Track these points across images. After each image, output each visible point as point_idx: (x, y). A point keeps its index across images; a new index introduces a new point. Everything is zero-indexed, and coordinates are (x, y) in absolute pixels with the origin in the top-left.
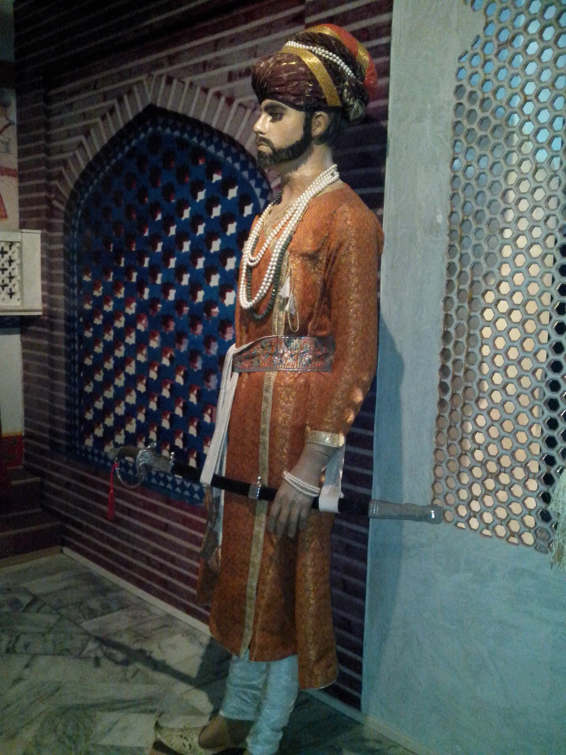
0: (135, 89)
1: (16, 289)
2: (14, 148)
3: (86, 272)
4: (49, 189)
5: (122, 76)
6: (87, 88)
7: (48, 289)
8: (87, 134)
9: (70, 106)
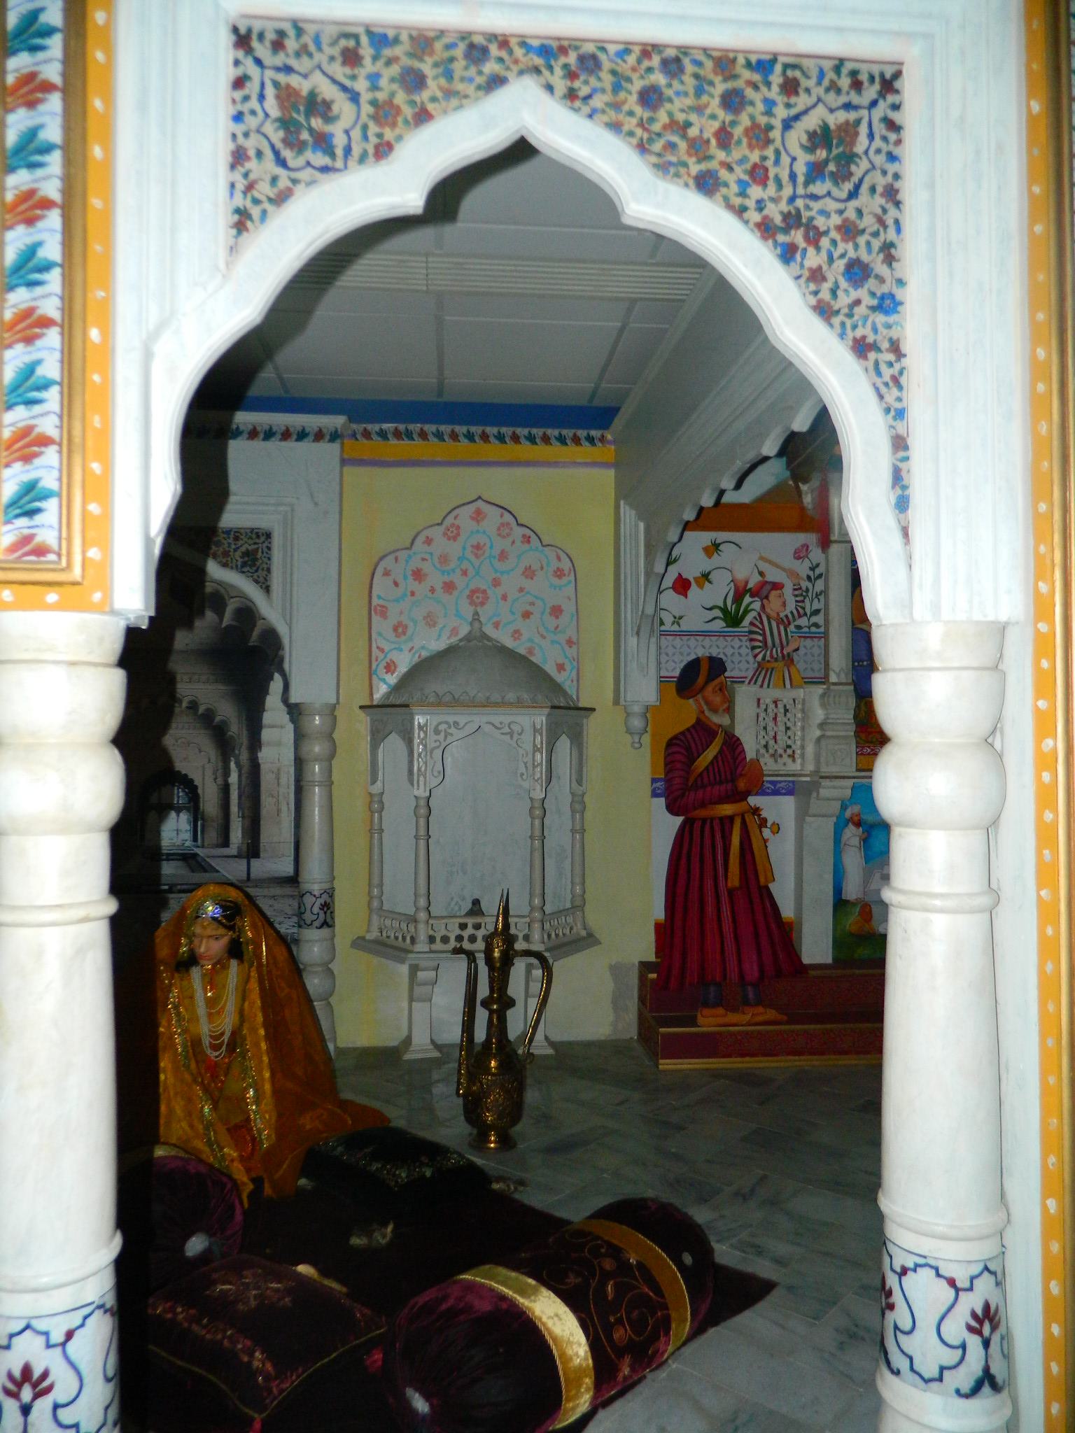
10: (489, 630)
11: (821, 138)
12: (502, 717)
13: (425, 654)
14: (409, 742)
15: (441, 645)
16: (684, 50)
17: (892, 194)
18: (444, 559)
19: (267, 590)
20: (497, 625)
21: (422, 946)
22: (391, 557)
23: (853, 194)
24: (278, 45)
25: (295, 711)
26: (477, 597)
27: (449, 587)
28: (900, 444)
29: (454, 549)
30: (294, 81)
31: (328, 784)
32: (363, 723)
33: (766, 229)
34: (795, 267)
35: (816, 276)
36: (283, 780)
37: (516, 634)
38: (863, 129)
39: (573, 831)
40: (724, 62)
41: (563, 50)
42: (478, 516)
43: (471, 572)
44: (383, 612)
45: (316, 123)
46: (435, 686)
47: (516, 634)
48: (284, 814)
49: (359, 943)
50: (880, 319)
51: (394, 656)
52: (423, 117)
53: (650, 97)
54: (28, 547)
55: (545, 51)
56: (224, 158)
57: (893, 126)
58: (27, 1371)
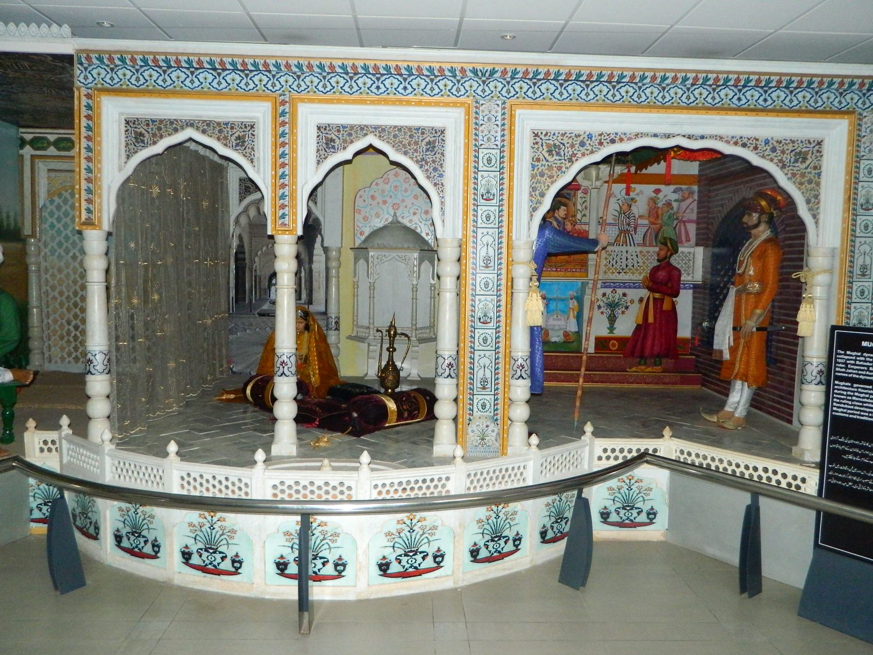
9: (717, 195)
10: (400, 219)
12: (402, 253)
13: (375, 228)
14: (367, 262)
15: (381, 225)
17: (443, 154)
19: (316, 203)
20: (403, 218)
21: (371, 337)
25: (326, 250)
26: (396, 206)
27: (385, 202)
29: (387, 187)
32: (351, 254)
33: (417, 162)
35: (427, 170)
37: (411, 221)
40: (410, 129)
44: (359, 212)
46: (378, 241)
47: (411, 221)
49: (350, 338)
51: (363, 229)
52: (352, 142)
53: (395, 136)
54: (284, 224)
55: (375, 128)
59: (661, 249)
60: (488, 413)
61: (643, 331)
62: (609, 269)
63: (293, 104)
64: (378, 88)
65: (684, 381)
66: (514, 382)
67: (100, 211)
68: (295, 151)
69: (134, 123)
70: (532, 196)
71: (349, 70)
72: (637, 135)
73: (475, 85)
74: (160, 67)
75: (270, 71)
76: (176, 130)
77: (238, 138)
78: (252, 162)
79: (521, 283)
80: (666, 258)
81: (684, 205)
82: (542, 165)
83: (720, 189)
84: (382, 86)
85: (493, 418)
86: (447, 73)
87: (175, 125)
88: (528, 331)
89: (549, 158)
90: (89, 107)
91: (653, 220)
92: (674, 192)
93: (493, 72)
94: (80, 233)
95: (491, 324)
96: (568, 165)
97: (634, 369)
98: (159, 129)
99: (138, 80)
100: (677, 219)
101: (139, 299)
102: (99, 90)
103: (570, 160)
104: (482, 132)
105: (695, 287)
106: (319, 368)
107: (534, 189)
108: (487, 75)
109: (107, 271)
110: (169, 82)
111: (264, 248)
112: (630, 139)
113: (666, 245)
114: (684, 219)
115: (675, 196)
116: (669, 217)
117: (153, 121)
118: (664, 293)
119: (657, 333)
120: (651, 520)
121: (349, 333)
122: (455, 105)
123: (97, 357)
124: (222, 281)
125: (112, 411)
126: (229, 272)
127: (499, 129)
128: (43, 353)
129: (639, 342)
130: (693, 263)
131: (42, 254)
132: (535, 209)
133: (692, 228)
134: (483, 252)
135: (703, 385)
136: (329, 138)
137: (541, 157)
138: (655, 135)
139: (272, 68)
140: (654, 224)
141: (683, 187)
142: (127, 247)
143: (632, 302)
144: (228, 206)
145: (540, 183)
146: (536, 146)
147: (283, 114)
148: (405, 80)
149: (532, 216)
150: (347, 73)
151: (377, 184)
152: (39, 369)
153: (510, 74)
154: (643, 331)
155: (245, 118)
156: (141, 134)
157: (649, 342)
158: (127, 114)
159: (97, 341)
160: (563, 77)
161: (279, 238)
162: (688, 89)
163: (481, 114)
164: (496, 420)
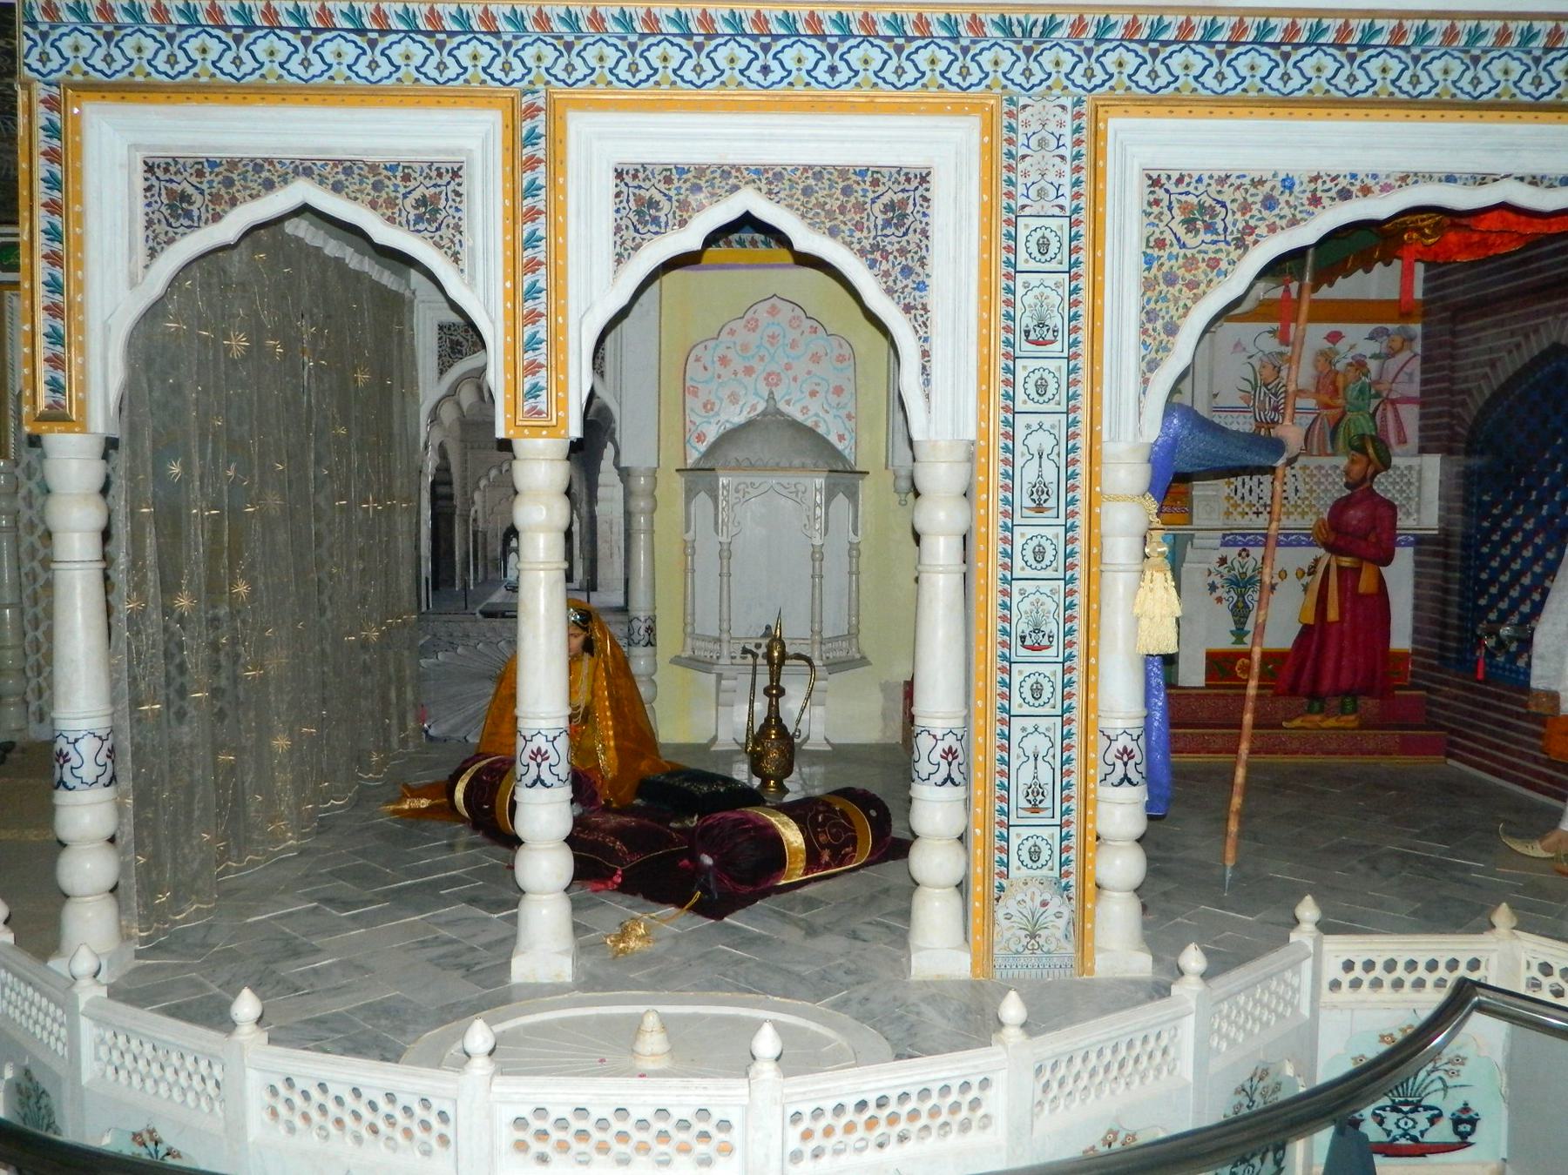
0: (1542, 330)
1: (1413, 509)
2: (1417, 378)
3: (1486, 493)
4: (1452, 415)
5: (1528, 317)
6: (1495, 325)
7: (1446, 509)
8: (1493, 364)
9: (1477, 341)
10: (782, 406)
11: (890, 207)
12: (789, 479)
13: (729, 426)
15: (739, 419)
16: (824, 167)
18: (745, 348)
20: (788, 403)
21: (725, 660)
22: (701, 346)
23: (905, 234)
24: (635, 177)
25: (625, 474)
26: (772, 379)
27: (749, 371)
28: (925, 354)
29: (753, 338)
30: (642, 192)
31: (651, 532)
32: (679, 483)
33: (862, 253)
34: (876, 271)
35: (887, 274)
36: (615, 529)
38: (911, 201)
39: (850, 573)
40: (843, 172)
41: (766, 171)
42: (773, 311)
43: (767, 358)
45: (652, 212)
46: (736, 454)
47: (805, 410)
48: (616, 557)
49: (677, 661)
50: (917, 293)
51: (704, 428)
53: (807, 191)
55: (757, 172)
56: (612, 230)
57: (926, 199)
58: (539, 749)
59: (1353, 462)
60: (1045, 871)
61: (1316, 637)
62: (1236, 506)
63: (554, 111)
64: (765, 70)
65: (1407, 748)
66: (1107, 792)
67: (83, 386)
68: (559, 229)
69: (166, 170)
70: (1145, 332)
71: (694, 27)
72: (1404, 179)
73: (1007, 59)
74: (227, 28)
75: (497, 34)
76: (269, 185)
77: (422, 202)
78: (456, 261)
79: (1120, 548)
80: (1364, 479)
81: (1393, 365)
82: (1170, 257)
83: (1483, 329)
84: (774, 65)
85: (1058, 882)
86: (937, 30)
87: (265, 173)
88: (1140, 665)
89: (1189, 239)
90: (53, 131)
91: (1326, 399)
92: (1371, 338)
93: (1050, 27)
94: (35, 441)
95: (1052, 651)
96: (1234, 255)
97: (1297, 722)
98: (229, 183)
99: (172, 60)
100: (1378, 395)
101: (195, 595)
102: (76, 87)
103: (1241, 244)
104: (1025, 175)
105: (1419, 542)
106: (616, 736)
107: (1151, 316)
108: (1036, 32)
109: (106, 535)
110: (249, 64)
111: (493, 473)
112: (1386, 188)
113: (1362, 450)
114: (1393, 396)
115: (1374, 347)
116: (1361, 391)
117: (213, 164)
118: (1362, 558)
119: (1346, 643)
120: (1464, 1136)
121: (676, 650)
122: (958, 109)
123: (81, 746)
124: (403, 544)
125: (124, 869)
126: (418, 523)
127: (1067, 168)
128: (26, 703)
129: (1309, 664)
130: (1422, 489)
131: (23, 492)
132: (1153, 365)
133: (1411, 416)
134: (1030, 475)
135: (1450, 755)
136: (644, 198)
137: (1168, 236)
138: (1450, 179)
139: (502, 25)
140: (1327, 407)
141: (1389, 326)
142: (159, 474)
143: (1283, 575)
144: (414, 383)
145: (1165, 299)
146: (1156, 210)
147: (532, 138)
148: (833, 48)
149: (1146, 381)
150: (688, 35)
151: (732, 332)
152: (16, 738)
153: (1092, 30)
154: (1316, 637)
155: (438, 151)
156: (184, 197)
157: (1330, 665)
158: (149, 147)
159: (83, 704)
160: (1224, 35)
161: (522, 445)
162: (1537, 60)
163: (1021, 130)
164: (1067, 888)
